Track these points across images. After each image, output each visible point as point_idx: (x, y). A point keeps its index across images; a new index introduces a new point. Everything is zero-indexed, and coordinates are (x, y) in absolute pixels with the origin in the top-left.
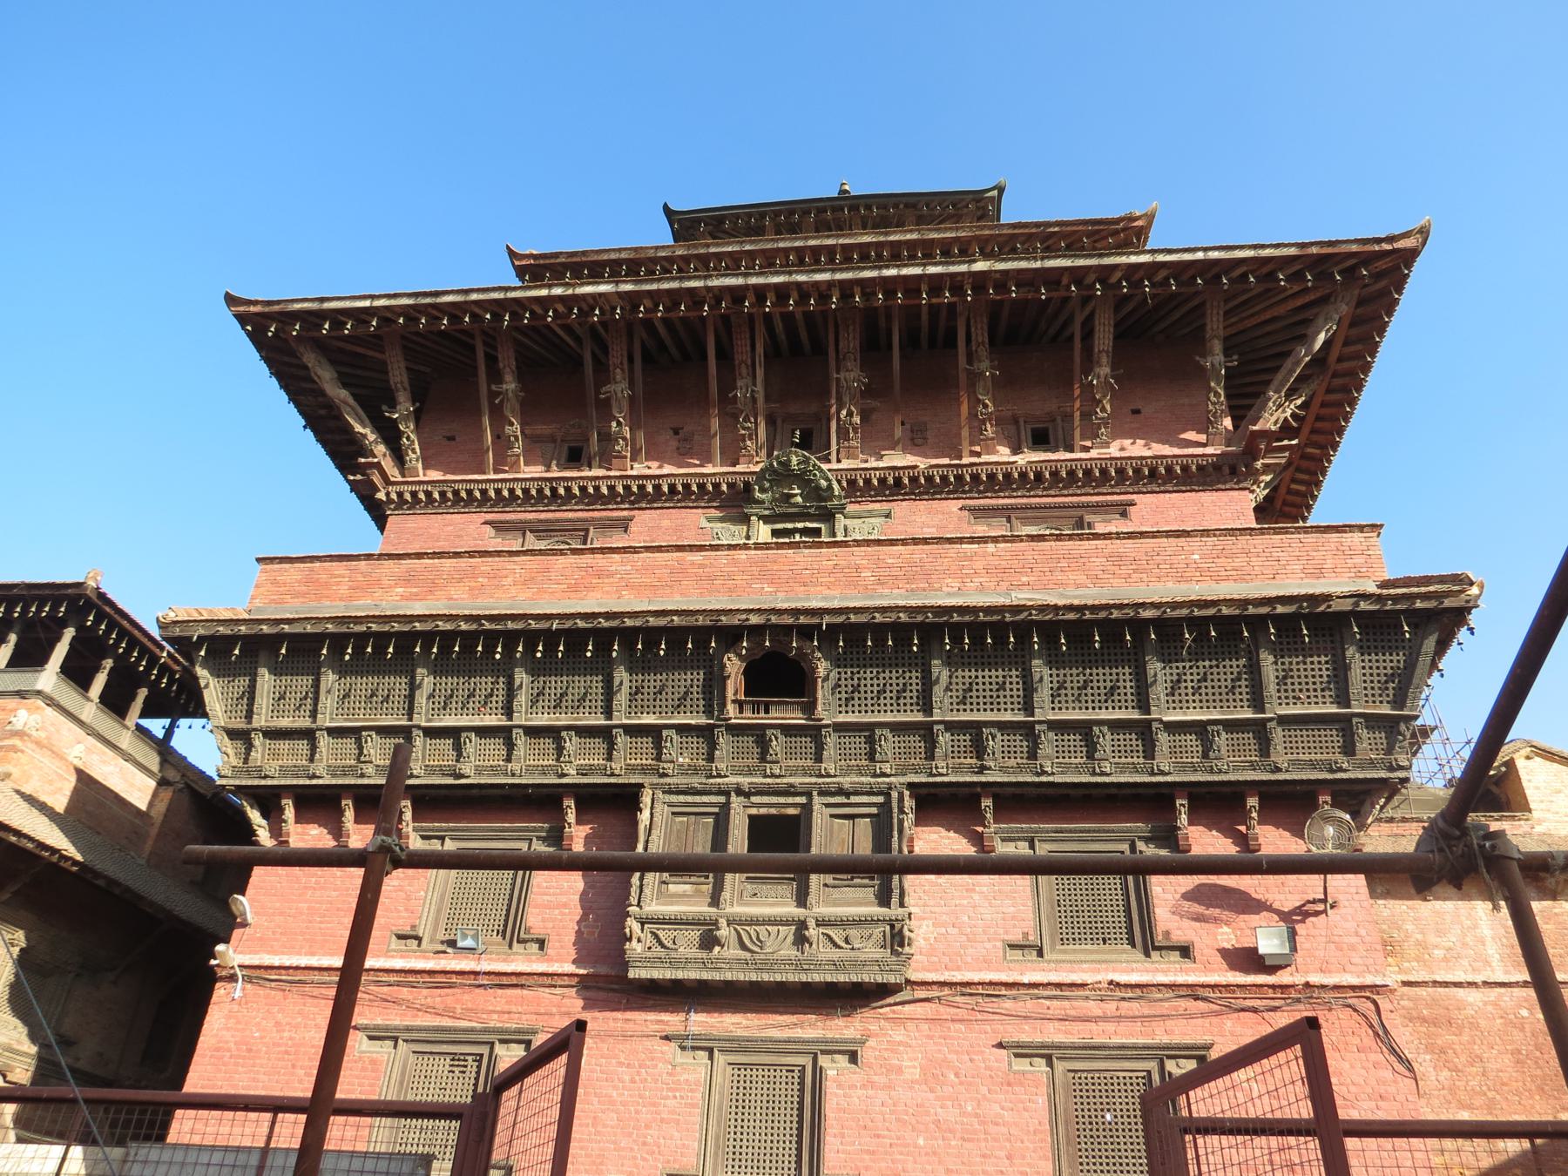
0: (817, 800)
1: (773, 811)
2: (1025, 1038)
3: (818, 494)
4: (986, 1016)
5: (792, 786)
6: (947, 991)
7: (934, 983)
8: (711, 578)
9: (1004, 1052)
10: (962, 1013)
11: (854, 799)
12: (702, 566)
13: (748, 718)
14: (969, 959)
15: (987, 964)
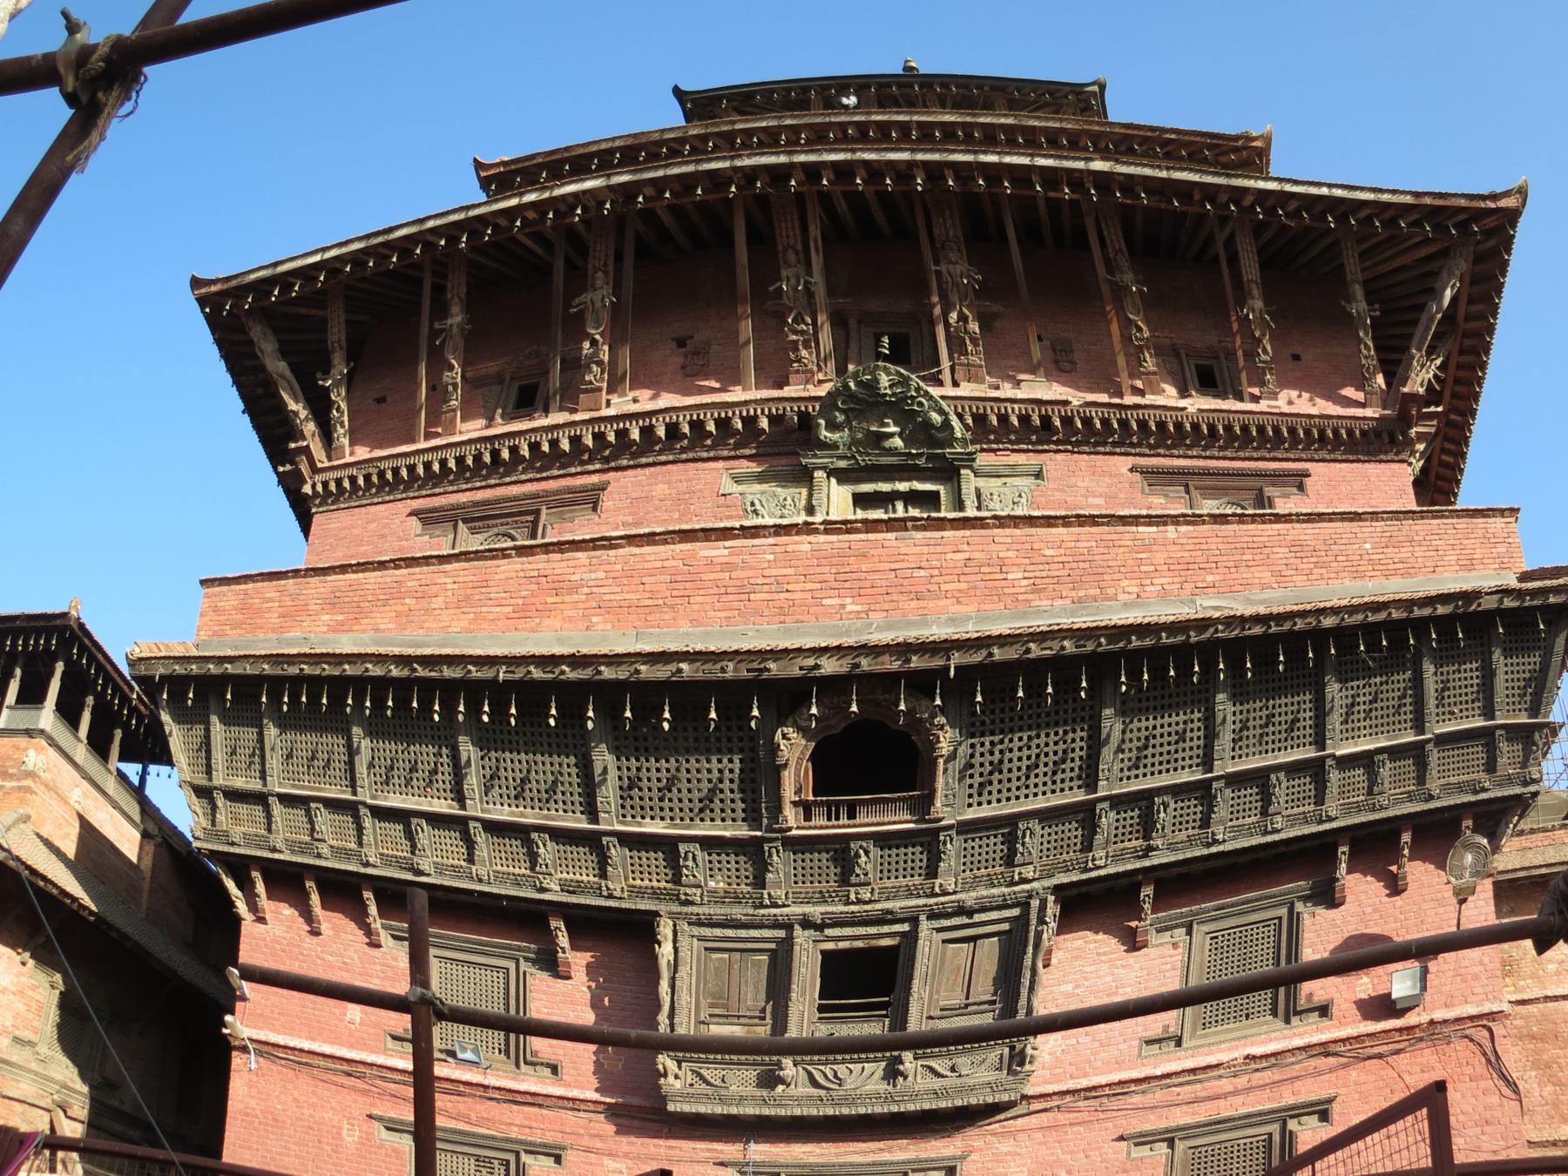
0: (925, 925)
1: (859, 944)
2: (1148, 1127)
3: (924, 433)
4: (1109, 1114)
5: (889, 912)
6: (1068, 1098)
7: (1055, 1094)
8: (745, 591)
9: (1124, 1144)
10: (1085, 1116)
11: (977, 918)
12: (728, 567)
13: (820, 826)
14: (1099, 1064)
15: (1119, 1064)
